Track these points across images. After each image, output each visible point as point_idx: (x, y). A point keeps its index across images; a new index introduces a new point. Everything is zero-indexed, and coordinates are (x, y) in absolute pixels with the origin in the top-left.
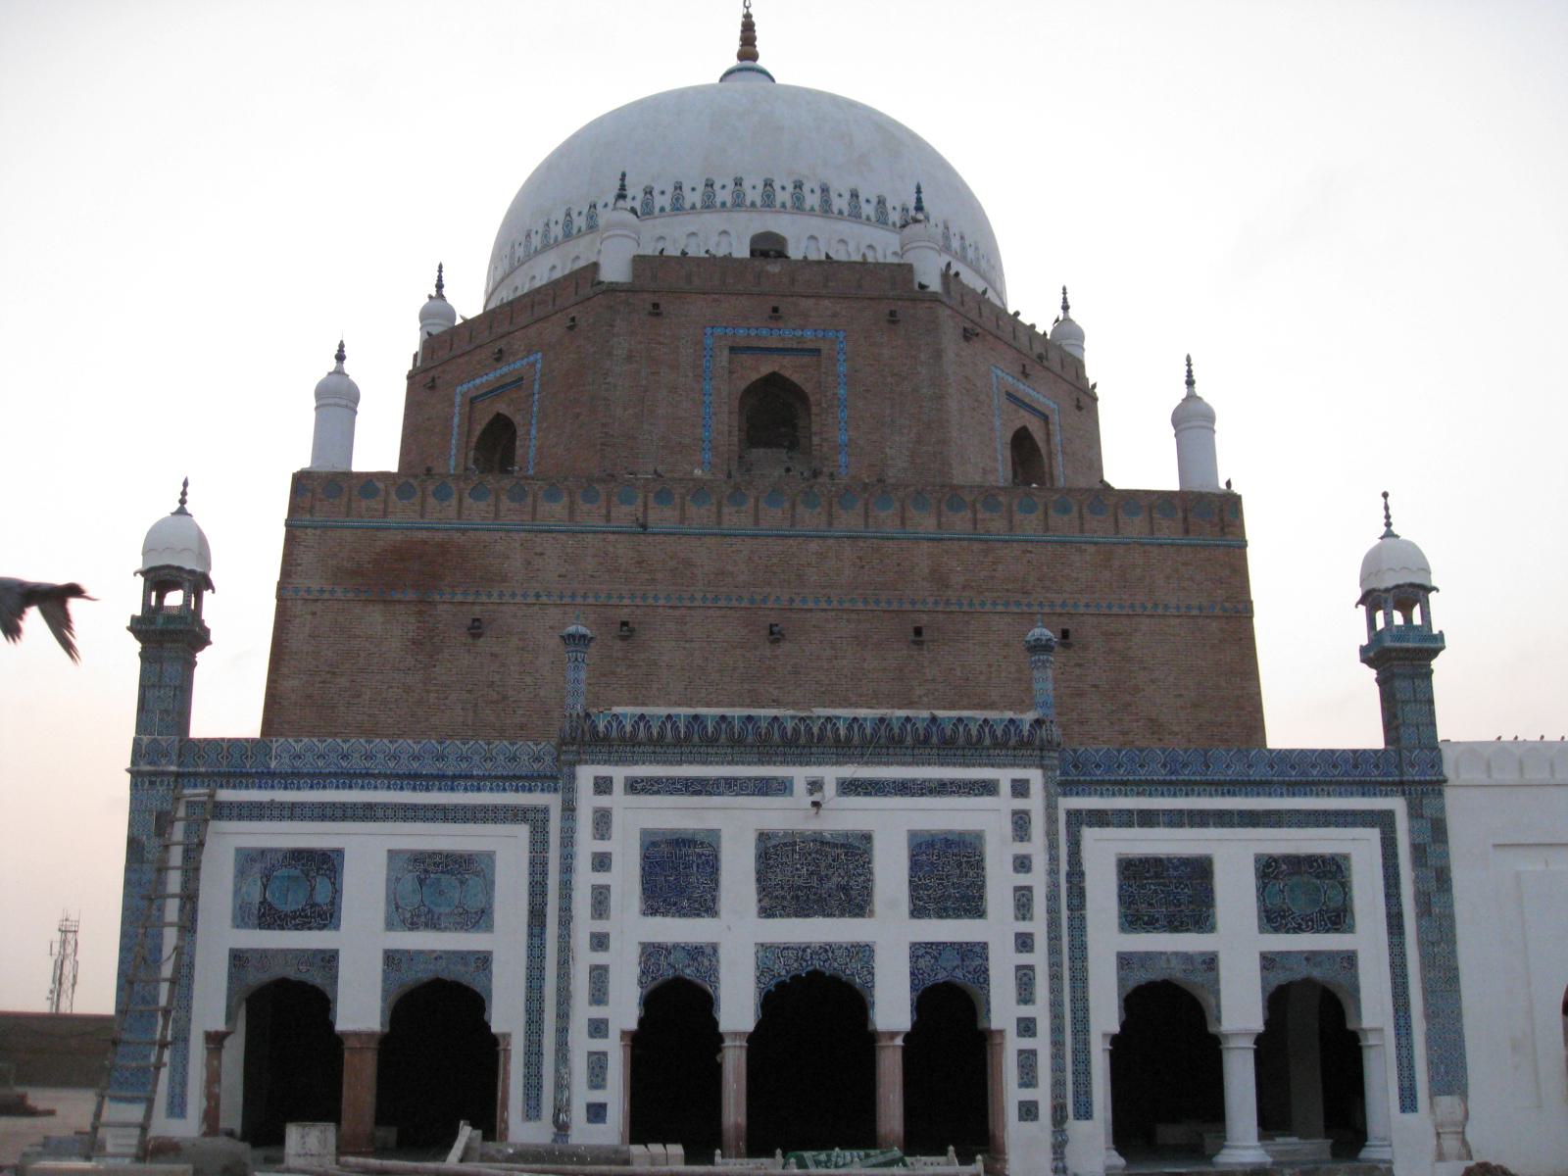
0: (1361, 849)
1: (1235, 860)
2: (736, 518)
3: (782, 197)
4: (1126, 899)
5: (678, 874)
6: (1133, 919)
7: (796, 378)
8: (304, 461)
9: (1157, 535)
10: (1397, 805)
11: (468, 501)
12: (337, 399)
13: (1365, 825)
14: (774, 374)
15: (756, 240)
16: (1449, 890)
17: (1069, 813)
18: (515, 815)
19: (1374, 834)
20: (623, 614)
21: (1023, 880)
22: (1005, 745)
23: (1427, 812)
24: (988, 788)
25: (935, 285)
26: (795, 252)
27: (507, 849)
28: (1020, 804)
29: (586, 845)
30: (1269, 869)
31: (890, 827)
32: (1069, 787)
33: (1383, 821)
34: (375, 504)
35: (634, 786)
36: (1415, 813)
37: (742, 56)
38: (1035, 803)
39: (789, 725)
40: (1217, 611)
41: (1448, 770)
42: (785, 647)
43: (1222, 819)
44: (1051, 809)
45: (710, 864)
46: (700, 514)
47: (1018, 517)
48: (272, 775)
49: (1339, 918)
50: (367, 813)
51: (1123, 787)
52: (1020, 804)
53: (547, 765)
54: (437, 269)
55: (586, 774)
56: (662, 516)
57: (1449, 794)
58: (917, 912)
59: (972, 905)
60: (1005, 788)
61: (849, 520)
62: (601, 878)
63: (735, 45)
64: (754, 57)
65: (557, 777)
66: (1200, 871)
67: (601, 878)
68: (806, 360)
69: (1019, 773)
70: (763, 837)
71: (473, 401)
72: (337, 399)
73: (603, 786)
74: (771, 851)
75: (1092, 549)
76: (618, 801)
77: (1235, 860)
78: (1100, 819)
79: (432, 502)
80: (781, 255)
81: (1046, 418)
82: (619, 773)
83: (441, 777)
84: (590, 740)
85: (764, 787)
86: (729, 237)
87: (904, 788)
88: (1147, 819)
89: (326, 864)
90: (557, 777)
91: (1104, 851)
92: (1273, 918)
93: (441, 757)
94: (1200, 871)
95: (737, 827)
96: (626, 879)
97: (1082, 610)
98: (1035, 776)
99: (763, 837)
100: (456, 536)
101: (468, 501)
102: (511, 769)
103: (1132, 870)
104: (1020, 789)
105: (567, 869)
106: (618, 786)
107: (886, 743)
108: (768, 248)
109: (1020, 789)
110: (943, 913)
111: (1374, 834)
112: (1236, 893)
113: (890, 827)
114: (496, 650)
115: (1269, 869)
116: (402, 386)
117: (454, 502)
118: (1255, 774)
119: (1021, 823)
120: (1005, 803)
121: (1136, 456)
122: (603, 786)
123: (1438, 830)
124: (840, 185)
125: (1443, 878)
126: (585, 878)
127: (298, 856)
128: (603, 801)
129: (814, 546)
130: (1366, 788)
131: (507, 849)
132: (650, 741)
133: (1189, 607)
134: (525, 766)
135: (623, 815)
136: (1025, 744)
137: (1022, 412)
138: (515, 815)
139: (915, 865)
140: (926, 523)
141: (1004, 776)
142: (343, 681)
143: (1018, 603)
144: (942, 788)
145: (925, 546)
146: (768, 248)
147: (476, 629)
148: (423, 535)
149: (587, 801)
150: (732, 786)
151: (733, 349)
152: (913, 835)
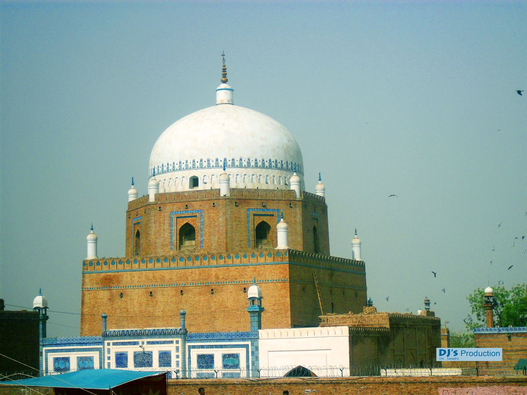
0: (242, 353)
1: (218, 354)
2: (173, 265)
3: (198, 165)
4: (198, 362)
5: (121, 359)
6: (200, 367)
7: (192, 224)
9: (267, 262)
10: (249, 343)
11: (118, 265)
13: (243, 347)
14: (187, 224)
16: (258, 360)
17: (189, 346)
18: (96, 349)
19: (244, 349)
20: (150, 290)
21: (178, 360)
22: (174, 334)
23: (255, 345)
24: (172, 342)
27: (96, 355)
28: (177, 345)
29: (107, 355)
30: (225, 356)
31: (155, 350)
32: (189, 341)
33: (247, 346)
34: (100, 267)
35: (114, 344)
36: (252, 345)
38: (180, 345)
39: (138, 331)
40: (280, 281)
41: (260, 336)
42: (184, 295)
43: (216, 347)
44: (184, 346)
45: (126, 358)
46: (166, 264)
47: (235, 260)
48: (58, 344)
49: (237, 366)
50: (73, 350)
51: (197, 341)
52: (177, 345)
53: (101, 341)
55: (106, 342)
56: (158, 265)
57: (259, 341)
58: (160, 366)
59: (169, 364)
60: (175, 342)
61: (198, 263)
62: (109, 361)
65: (102, 343)
66: (211, 357)
67: (109, 361)
68: (194, 218)
69: (177, 339)
70: (135, 353)
71: (135, 224)
73: (109, 344)
74: (136, 355)
75: (251, 267)
76: (111, 347)
77: (218, 354)
78: (194, 347)
79: (111, 266)
82: (111, 342)
83: (84, 343)
84: (106, 336)
85: (135, 343)
87: (158, 343)
88: (202, 347)
89: (67, 359)
90: (102, 343)
91: (195, 353)
92: (225, 366)
93: (84, 340)
94: (211, 357)
95: (130, 351)
96: (113, 362)
97: (249, 283)
98: (180, 340)
99: (135, 353)
100: (116, 273)
101: (118, 265)
102: (95, 341)
103: (200, 357)
104: (177, 342)
105: (104, 360)
106: (111, 344)
107: (154, 334)
109: (177, 342)
110: (164, 366)
111: (244, 349)
112: (218, 362)
113: (155, 350)
114: (126, 300)
115: (225, 356)
117: (115, 265)
118: (222, 338)
119: (177, 349)
120: (175, 345)
122: (109, 344)
123: (257, 348)
125: (257, 358)
126: (107, 361)
127: (63, 358)
128: (109, 347)
129: (190, 270)
130: (244, 340)
131: (96, 355)
132: (115, 336)
133: (273, 280)
134: (98, 341)
135: (113, 349)
136: (178, 334)
137: (262, 217)
138: (96, 349)
139: (160, 357)
140: (214, 262)
141: (175, 340)
142: (96, 309)
143: (234, 282)
144: (164, 343)
145: (214, 269)
147: (121, 295)
148: (109, 273)
149: (106, 347)
150: (130, 343)
152: (159, 351)
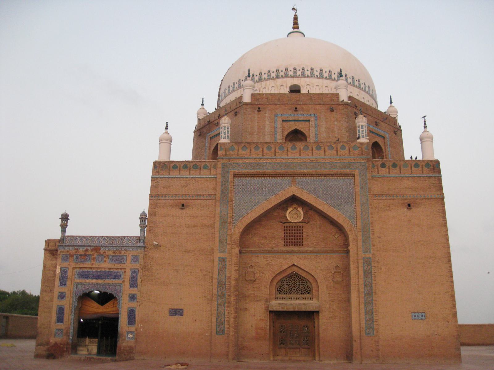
8: (156, 159)
12: (167, 141)
15: (291, 87)
25: (346, 100)
26: (303, 91)
37: (294, 28)
54: (202, 99)
63: (292, 25)
64: (298, 28)
72: (167, 141)
80: (299, 91)
81: (384, 138)
86: (281, 87)
108: (295, 90)
116: (192, 135)
121: (412, 150)
124: (317, 69)
146: (295, 90)
151: (284, 121)
